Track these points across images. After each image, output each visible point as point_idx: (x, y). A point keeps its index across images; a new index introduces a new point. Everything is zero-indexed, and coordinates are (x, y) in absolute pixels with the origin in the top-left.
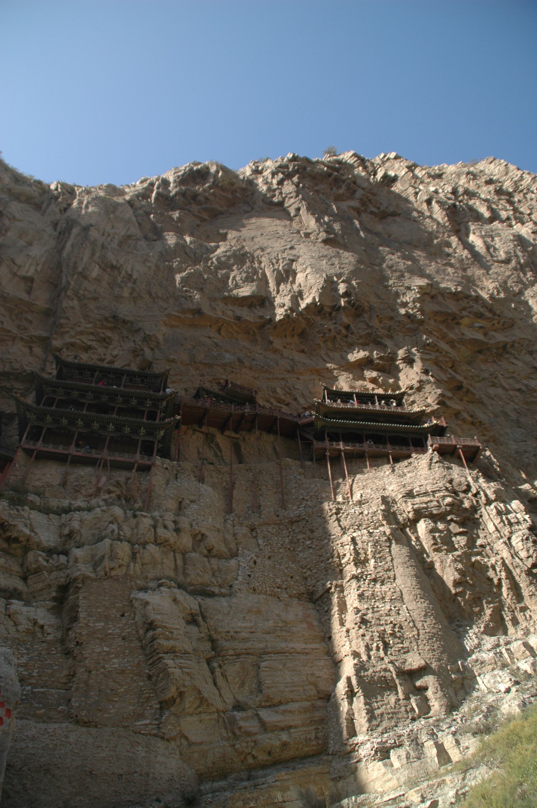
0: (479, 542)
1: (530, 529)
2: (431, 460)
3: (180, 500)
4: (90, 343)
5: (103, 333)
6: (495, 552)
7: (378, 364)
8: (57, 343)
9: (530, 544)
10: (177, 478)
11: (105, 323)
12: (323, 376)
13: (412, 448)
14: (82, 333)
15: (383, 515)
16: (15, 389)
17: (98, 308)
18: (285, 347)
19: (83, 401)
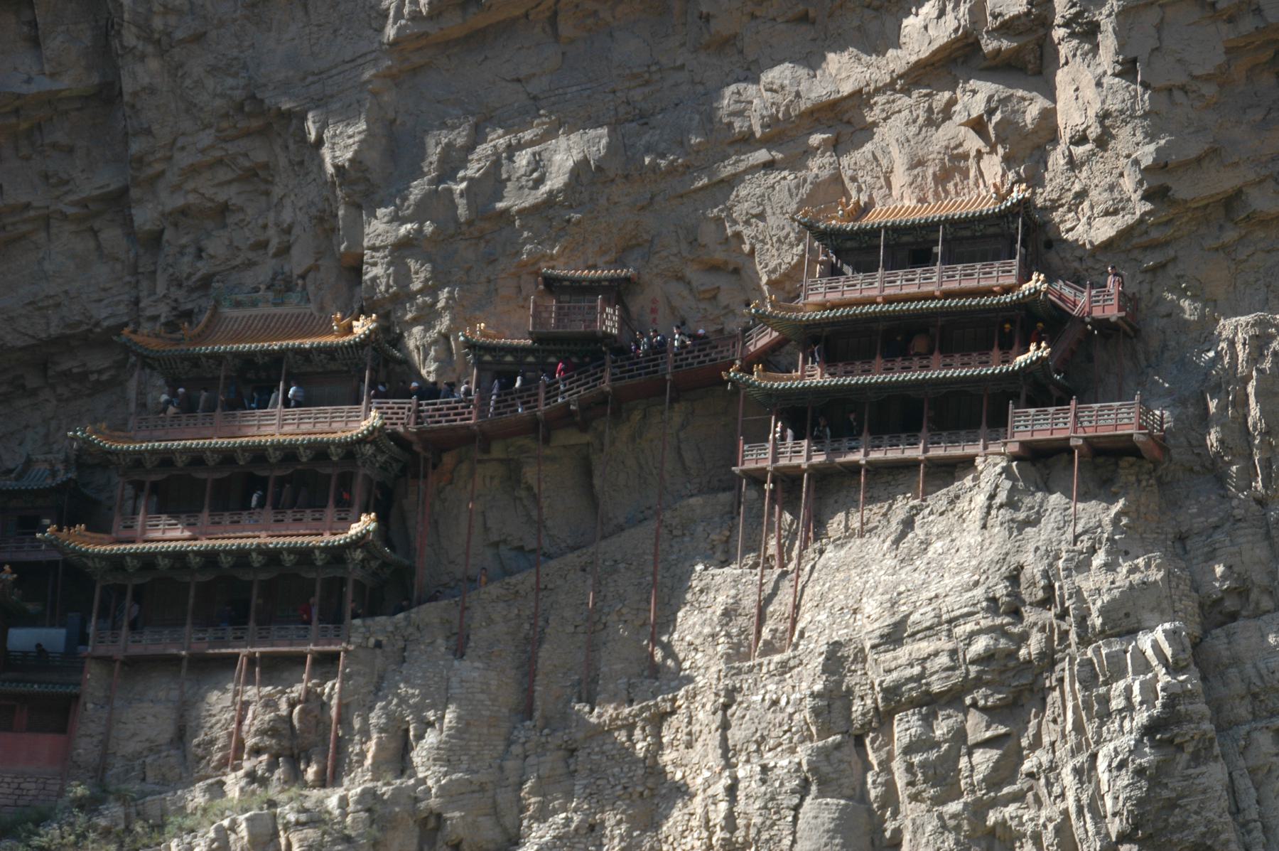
0: (1027, 766)
1: (1149, 730)
2: (992, 497)
3: (404, 727)
4: (222, 196)
5: (246, 155)
6: (1057, 790)
7: (998, 51)
8: (145, 216)
9: (1125, 779)
10: (404, 661)
11: (242, 124)
12: (849, 122)
13: (984, 429)
14: (194, 170)
15: (816, 712)
16: (92, 372)
17: (213, 70)
18: (753, 16)
19: (201, 475)
